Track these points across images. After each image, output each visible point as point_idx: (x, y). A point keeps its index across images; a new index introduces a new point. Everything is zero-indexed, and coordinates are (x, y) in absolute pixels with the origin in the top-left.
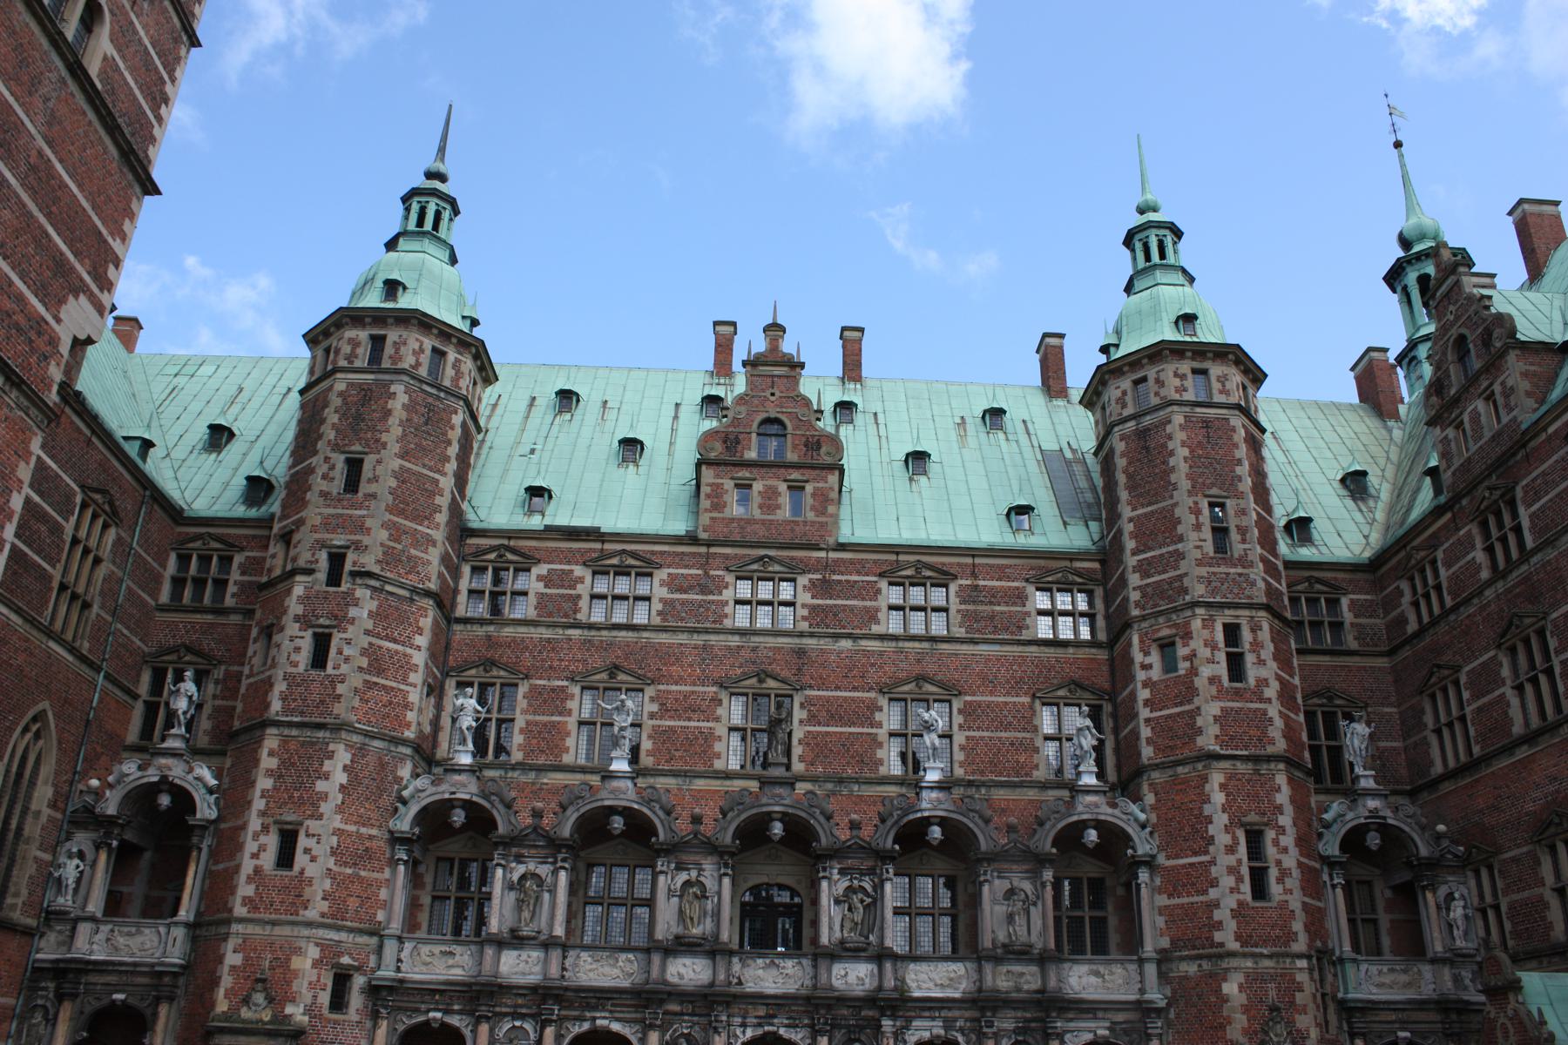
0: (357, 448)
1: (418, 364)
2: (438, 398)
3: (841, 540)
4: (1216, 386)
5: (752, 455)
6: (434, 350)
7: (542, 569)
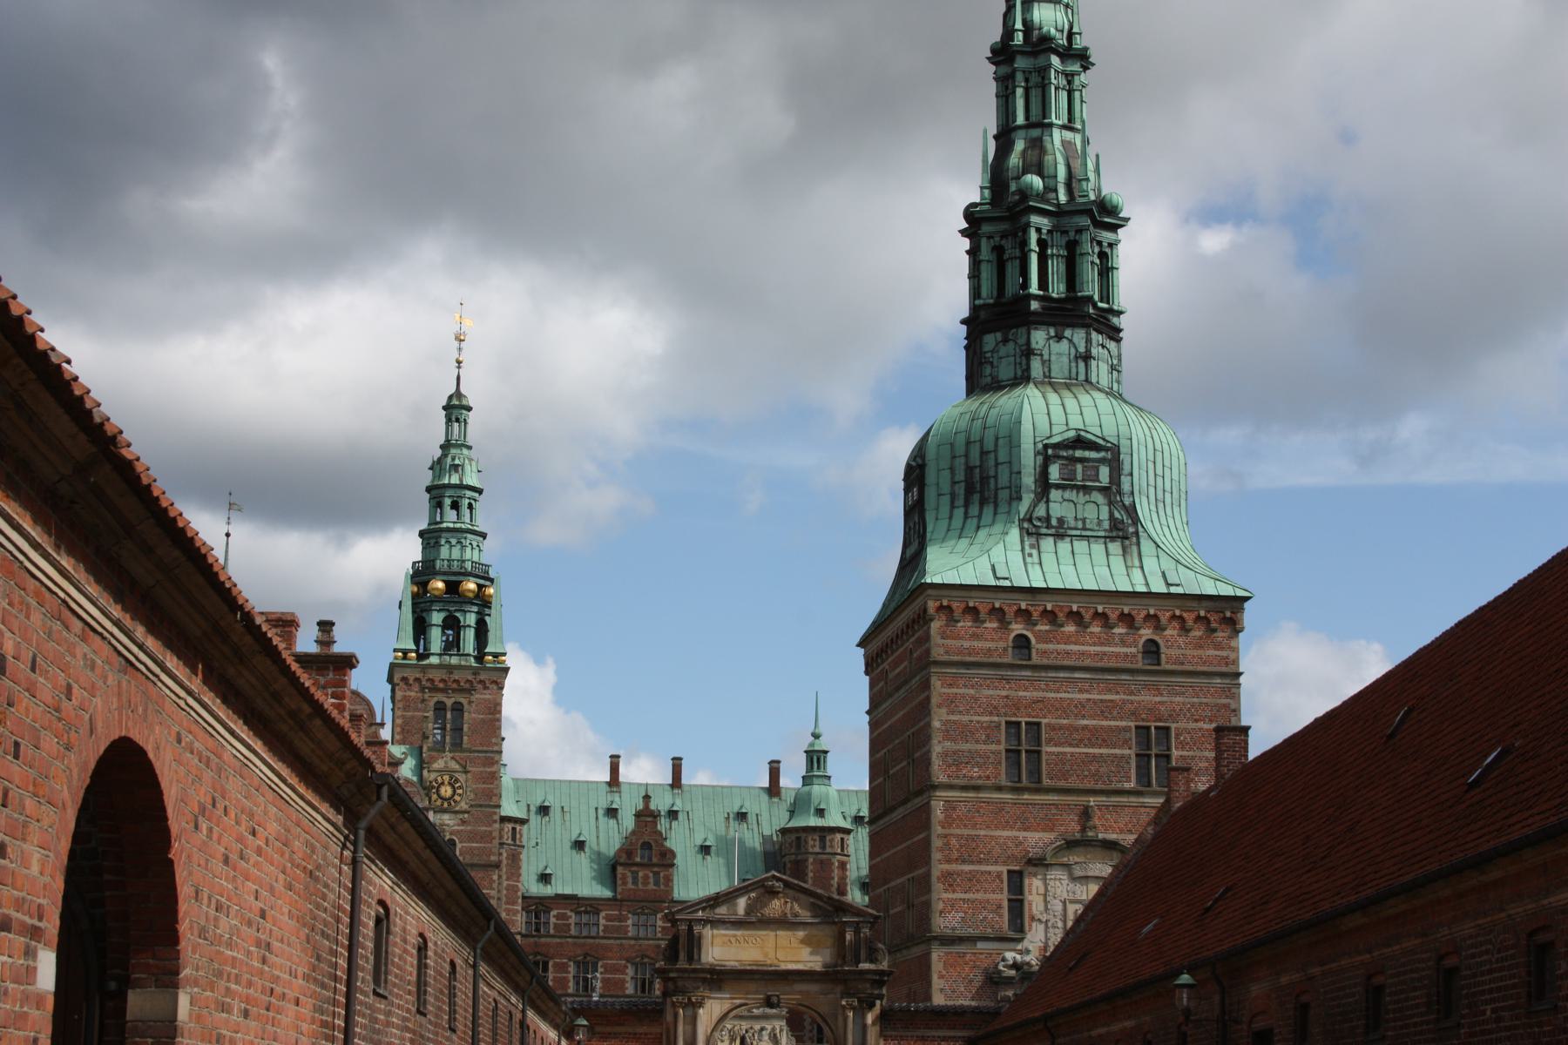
3: (675, 899)
4: (828, 844)
5: (638, 860)
7: (554, 913)
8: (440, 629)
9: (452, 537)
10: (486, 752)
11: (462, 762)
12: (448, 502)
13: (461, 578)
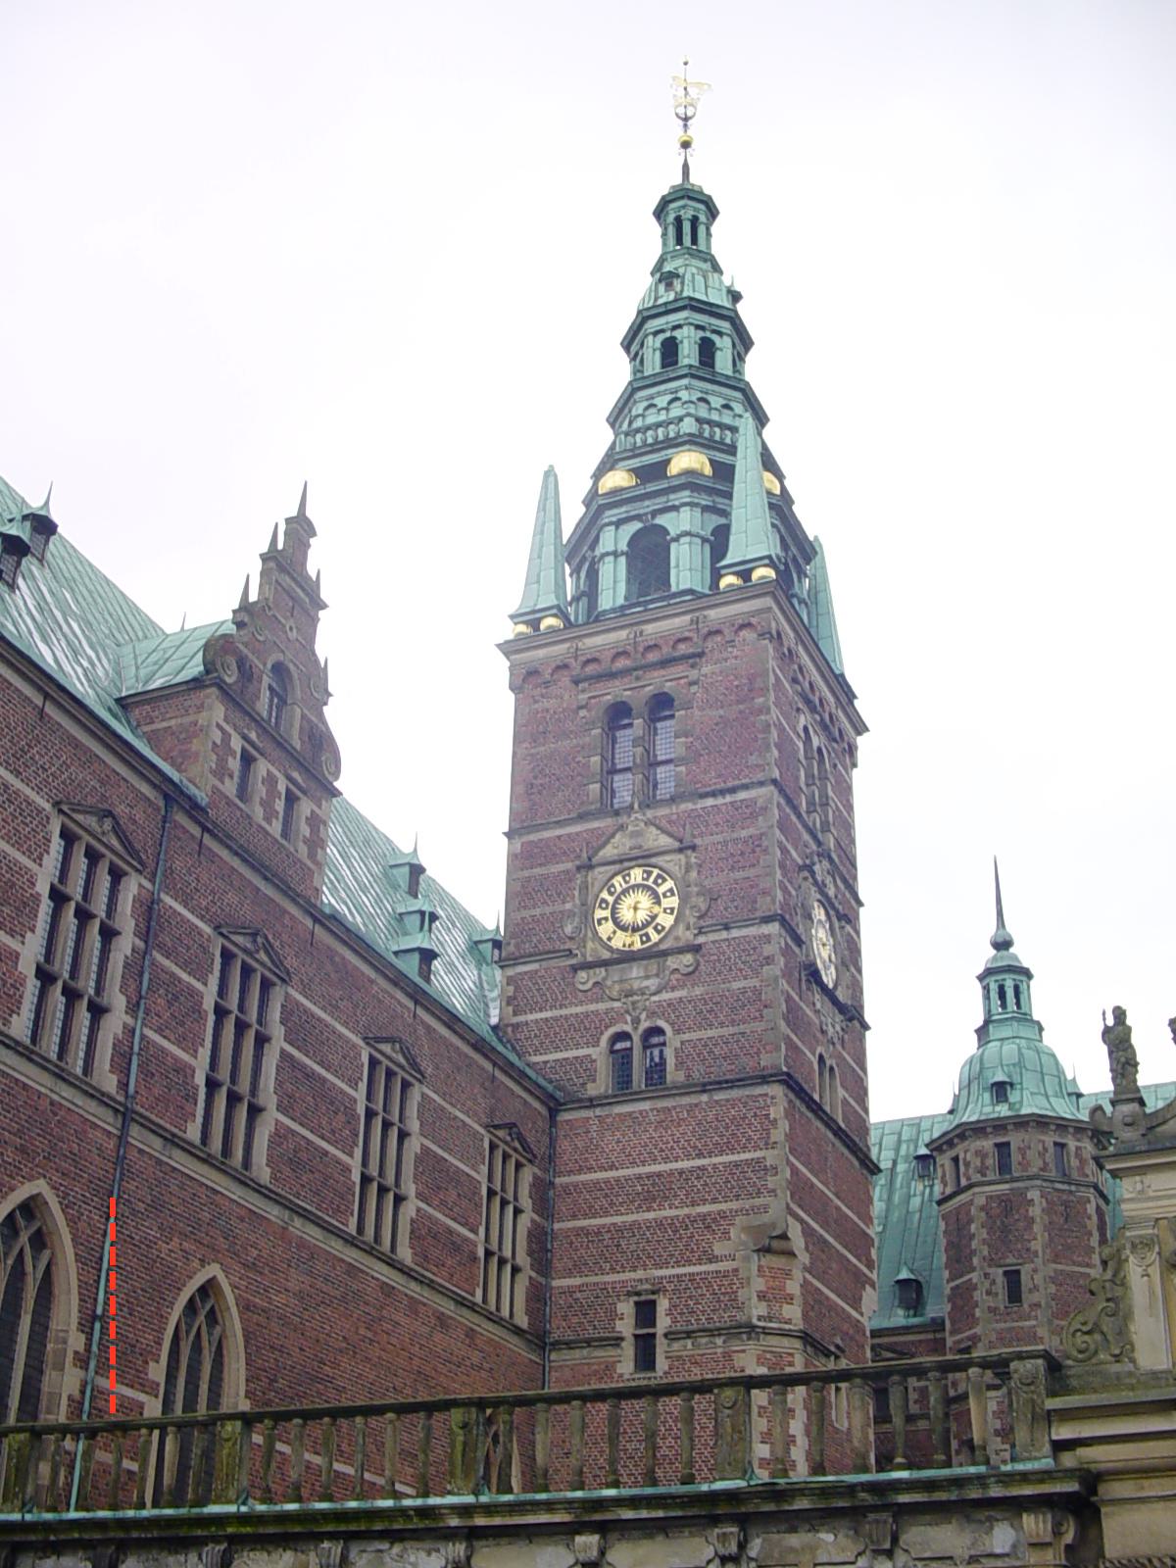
0: (1011, 1260)
1: (1045, 1164)
2: (1071, 1192)
6: (1056, 1144)
8: (623, 560)
9: (659, 394)
10: (733, 790)
11: (673, 829)
12: (654, 344)
13: (670, 451)
